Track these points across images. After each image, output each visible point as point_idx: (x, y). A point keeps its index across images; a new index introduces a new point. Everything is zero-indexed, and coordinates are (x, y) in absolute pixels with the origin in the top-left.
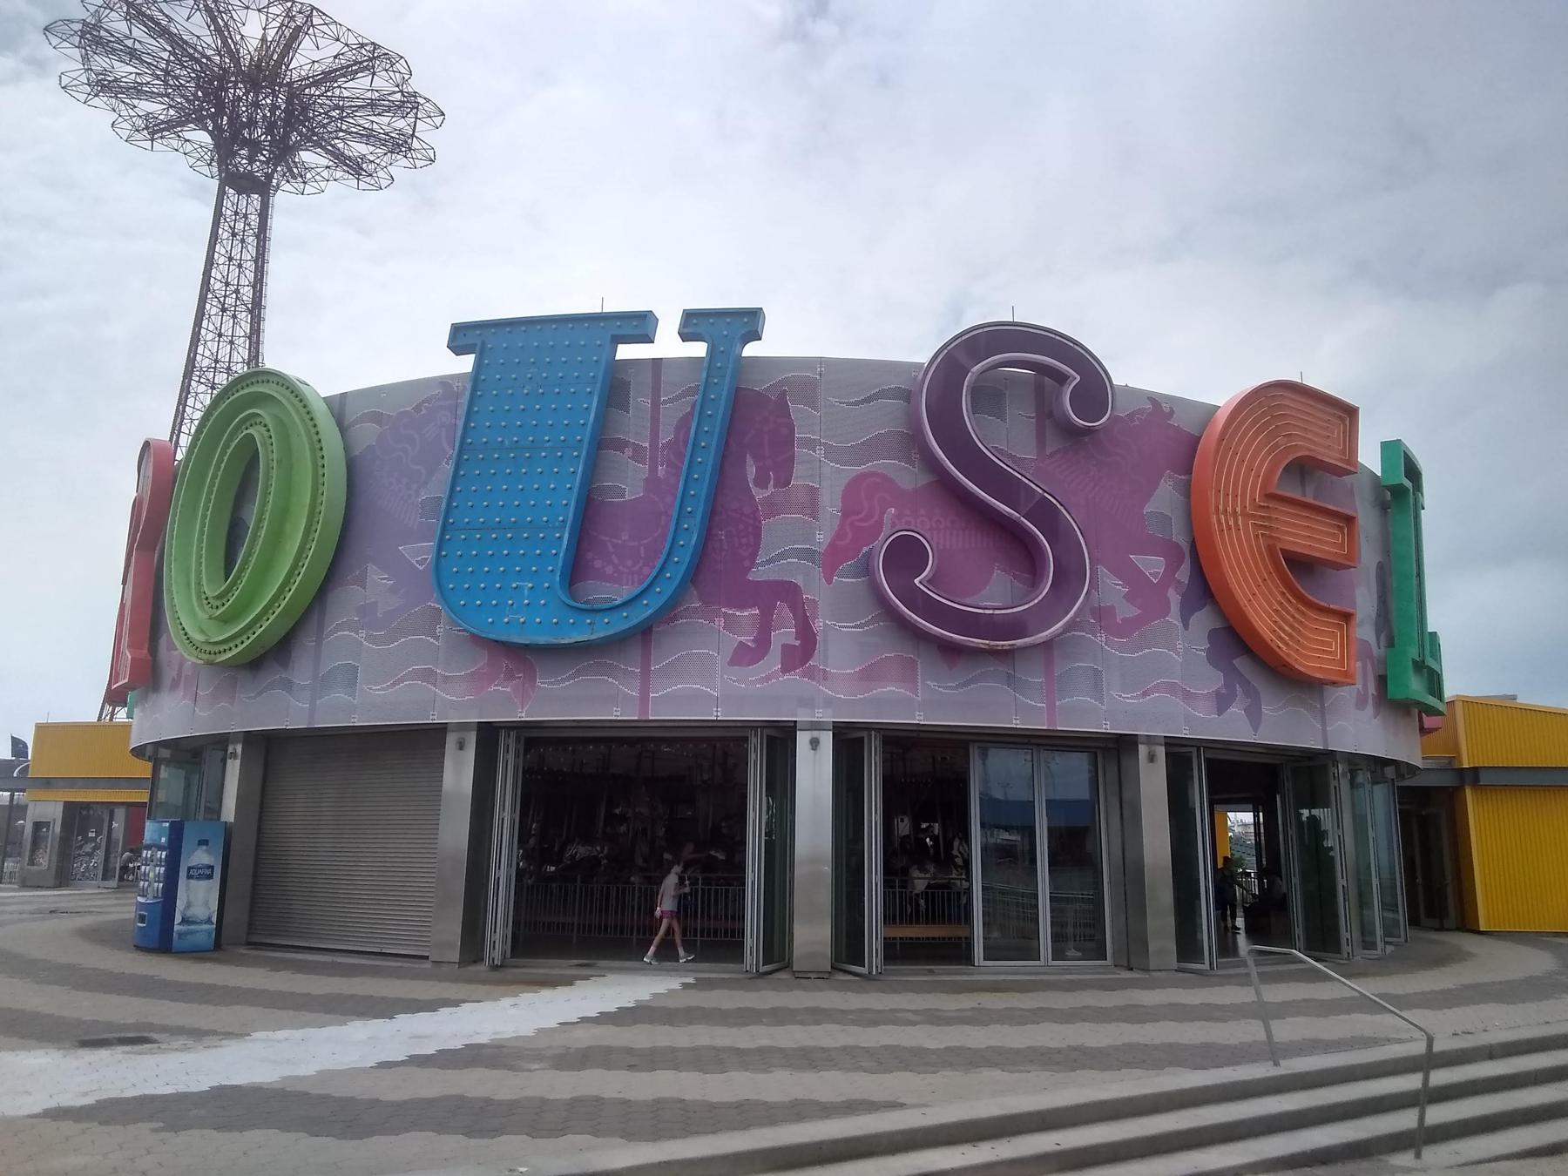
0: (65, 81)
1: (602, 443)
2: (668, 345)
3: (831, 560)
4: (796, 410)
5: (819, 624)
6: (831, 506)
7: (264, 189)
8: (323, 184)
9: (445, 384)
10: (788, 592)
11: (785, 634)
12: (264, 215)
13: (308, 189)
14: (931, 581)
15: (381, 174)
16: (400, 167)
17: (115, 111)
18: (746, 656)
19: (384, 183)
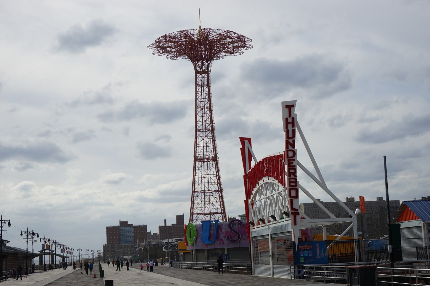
0: (153, 53)
1: (210, 229)
2: (213, 222)
3: (225, 237)
4: (222, 226)
5: (224, 241)
6: (224, 233)
7: (207, 73)
8: (225, 57)
9: (201, 225)
10: (222, 239)
11: (222, 242)
12: (208, 80)
13: (220, 58)
14: (230, 238)
15: (240, 52)
16: (244, 50)
17: (166, 55)
18: (220, 244)
19: (241, 53)
